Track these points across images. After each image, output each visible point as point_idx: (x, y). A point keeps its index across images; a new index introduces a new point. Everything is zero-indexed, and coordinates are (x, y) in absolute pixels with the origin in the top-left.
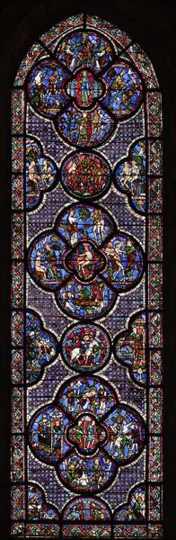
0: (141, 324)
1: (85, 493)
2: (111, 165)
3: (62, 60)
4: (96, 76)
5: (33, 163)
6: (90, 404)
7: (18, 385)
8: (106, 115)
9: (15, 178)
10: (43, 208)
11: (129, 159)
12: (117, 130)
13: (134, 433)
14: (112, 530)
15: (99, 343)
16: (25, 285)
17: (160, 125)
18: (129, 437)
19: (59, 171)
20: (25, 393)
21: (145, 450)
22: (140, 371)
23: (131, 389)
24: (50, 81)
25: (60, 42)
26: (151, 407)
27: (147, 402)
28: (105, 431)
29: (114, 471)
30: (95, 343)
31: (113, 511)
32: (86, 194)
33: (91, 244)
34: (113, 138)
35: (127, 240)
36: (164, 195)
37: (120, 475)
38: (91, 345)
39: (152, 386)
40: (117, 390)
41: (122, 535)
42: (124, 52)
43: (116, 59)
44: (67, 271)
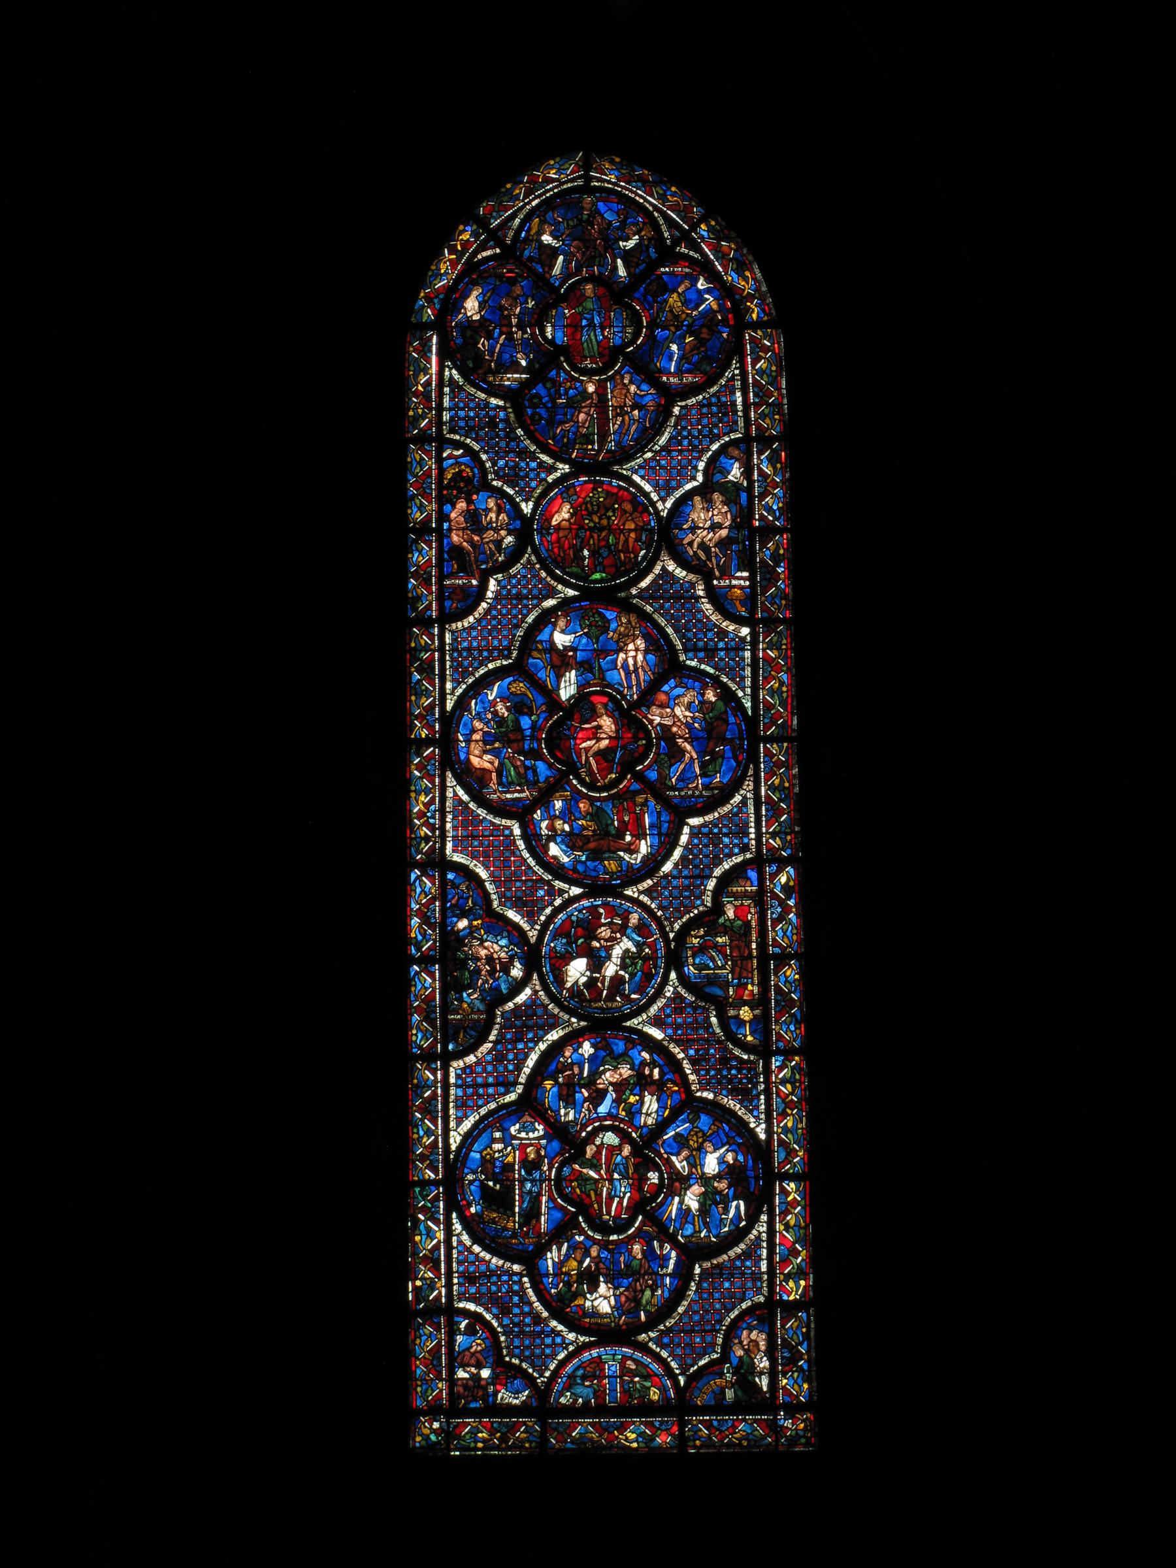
0: (745, 895)
1: (606, 1333)
2: (660, 506)
3: (531, 259)
4: (615, 295)
5: (462, 505)
6: (617, 1101)
7: (429, 1057)
8: (645, 387)
9: (416, 542)
10: (487, 612)
11: (704, 491)
12: (673, 420)
13: (730, 1172)
14: (681, 1431)
15: (638, 945)
16: (443, 798)
17: (780, 405)
19: (527, 521)
20: (446, 1076)
21: (764, 1218)
22: (745, 1013)
24: (502, 308)
25: (528, 218)
27: (768, 1092)
28: (657, 1168)
29: (683, 1274)
30: (627, 944)
31: (682, 1380)
32: (597, 576)
33: (612, 698)
34: (663, 440)
35: (705, 687)
36: (793, 573)
37: (699, 1285)
38: (617, 952)
39: (778, 1052)
40: (687, 1066)
41: (708, 1443)
42: (685, 237)
43: (668, 255)
44: (550, 766)
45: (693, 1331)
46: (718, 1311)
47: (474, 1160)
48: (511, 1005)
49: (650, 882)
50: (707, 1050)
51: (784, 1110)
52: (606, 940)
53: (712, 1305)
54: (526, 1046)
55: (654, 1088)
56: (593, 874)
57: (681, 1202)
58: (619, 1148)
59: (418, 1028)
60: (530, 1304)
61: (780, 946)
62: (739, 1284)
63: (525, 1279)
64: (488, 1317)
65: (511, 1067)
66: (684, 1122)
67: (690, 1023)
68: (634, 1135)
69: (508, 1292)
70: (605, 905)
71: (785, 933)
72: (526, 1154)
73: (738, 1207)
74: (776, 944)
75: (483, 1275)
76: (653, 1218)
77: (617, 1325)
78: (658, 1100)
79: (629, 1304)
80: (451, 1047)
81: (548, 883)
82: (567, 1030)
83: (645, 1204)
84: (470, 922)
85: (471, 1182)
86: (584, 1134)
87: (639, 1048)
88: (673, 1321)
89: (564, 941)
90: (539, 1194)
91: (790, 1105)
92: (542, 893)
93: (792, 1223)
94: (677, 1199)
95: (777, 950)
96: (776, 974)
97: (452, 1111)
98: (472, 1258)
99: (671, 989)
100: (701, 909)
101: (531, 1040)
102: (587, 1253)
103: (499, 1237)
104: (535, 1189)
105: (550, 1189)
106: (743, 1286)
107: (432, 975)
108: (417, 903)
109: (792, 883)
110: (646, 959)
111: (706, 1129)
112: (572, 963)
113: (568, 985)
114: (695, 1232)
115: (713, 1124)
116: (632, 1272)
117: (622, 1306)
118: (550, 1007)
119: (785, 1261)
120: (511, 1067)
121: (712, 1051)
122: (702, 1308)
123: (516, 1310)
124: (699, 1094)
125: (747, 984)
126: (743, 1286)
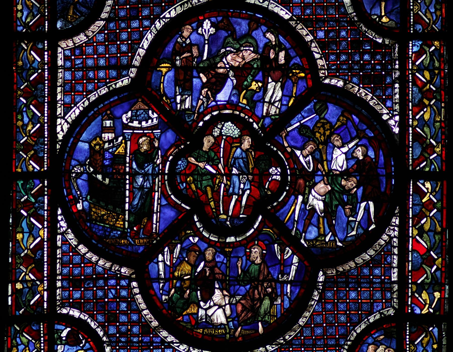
6: (238, 88)
7: (34, 36)
13: (357, 168)
18: (350, 184)
21: (396, 221)
23: (357, 44)
26: (413, 92)
27: (403, 81)
28: (279, 163)
29: (305, 281)
37: (322, 296)
39: (416, 36)
40: (315, 48)
45: (314, 345)
46: (343, 325)
47: (81, 150)
50: (339, 32)
51: (421, 101)
53: (336, 317)
54: (141, 25)
55: (278, 74)
57: (305, 202)
58: (240, 140)
60: (139, 311)
62: (366, 295)
63: (134, 284)
64: (93, 325)
65: (124, 48)
66: (310, 112)
68: (255, 125)
69: (115, 297)
72: (139, 145)
73: (367, 209)
75: (88, 278)
76: (274, 220)
77: (233, 337)
78: (282, 88)
79: (245, 315)
80: (59, 25)
83: (264, 204)
85: (79, 175)
86: (201, 124)
87: (264, 28)
88: (293, 334)
90: (152, 190)
91: (428, 95)
93: (427, 227)
94: (300, 198)
97: (59, 97)
98: (77, 259)
101: (147, 18)
102: (201, 256)
103: (108, 237)
104: (147, 184)
105: (163, 184)
106: (371, 296)
111: (334, 120)
114: (320, 235)
115: (342, 115)
116: (249, 278)
117: (238, 316)
119: (418, 270)
120: (124, 48)
121: (343, 33)
122: (325, 320)
123: (123, 318)
124: (327, 81)
126: (371, 296)
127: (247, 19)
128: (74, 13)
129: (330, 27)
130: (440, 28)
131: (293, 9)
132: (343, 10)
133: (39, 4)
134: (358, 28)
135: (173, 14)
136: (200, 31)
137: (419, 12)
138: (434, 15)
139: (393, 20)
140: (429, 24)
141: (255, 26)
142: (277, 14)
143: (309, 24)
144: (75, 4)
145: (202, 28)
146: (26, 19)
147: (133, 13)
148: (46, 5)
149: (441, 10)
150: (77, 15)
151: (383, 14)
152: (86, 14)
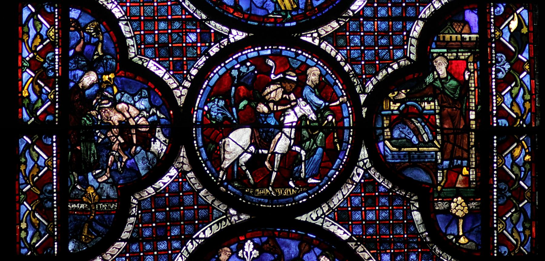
0: (462, 45)
15: (318, 110)
22: (459, 208)
30: (303, 109)
38: (290, 118)
48: (150, 190)
49: (335, 25)
52: (277, 103)
54: (170, 246)
56: (261, 12)
59: (30, 222)
61: (507, 116)
67: (385, 219)
70: (274, 56)
71: (514, 99)
74: (502, 113)
81: (201, 23)
82: (224, 225)
84: (100, 75)
87: (318, 251)
89: (222, 103)
92: (193, 37)
95: (503, 122)
96: (500, 154)
99: (361, 171)
100: (402, 63)
101: (177, 238)
107: (47, 150)
108: (31, 50)
109: (525, 30)
110: (328, 130)
112: (231, 136)
113: (226, 164)
118: (202, 193)
125: (461, 167)
127: (297, 240)
128: (89, 232)
129: (398, 249)
130: (529, 250)
131: (352, 228)
132: (412, 229)
133: (47, 221)
134: (431, 250)
135: (208, 234)
136: (240, 254)
137: (504, 231)
138: (522, 235)
139: (473, 241)
140: (516, 246)
141: (307, 248)
142: (333, 234)
143: (372, 246)
144: (90, 222)
145: (244, 250)
146: (31, 239)
147: (160, 233)
148: (55, 223)
149: (530, 229)
150: (92, 235)
151: (461, 234)
152: (103, 234)
